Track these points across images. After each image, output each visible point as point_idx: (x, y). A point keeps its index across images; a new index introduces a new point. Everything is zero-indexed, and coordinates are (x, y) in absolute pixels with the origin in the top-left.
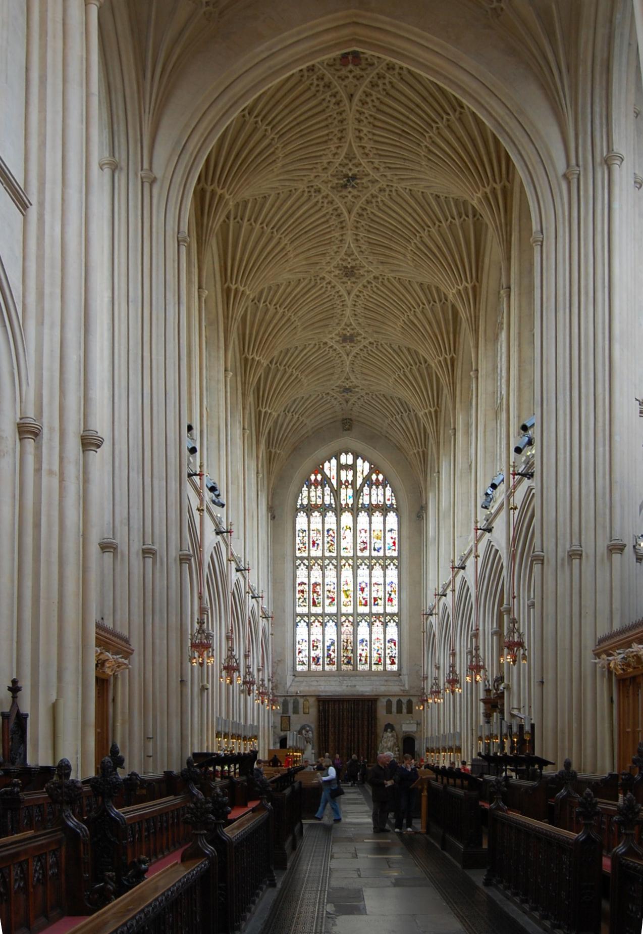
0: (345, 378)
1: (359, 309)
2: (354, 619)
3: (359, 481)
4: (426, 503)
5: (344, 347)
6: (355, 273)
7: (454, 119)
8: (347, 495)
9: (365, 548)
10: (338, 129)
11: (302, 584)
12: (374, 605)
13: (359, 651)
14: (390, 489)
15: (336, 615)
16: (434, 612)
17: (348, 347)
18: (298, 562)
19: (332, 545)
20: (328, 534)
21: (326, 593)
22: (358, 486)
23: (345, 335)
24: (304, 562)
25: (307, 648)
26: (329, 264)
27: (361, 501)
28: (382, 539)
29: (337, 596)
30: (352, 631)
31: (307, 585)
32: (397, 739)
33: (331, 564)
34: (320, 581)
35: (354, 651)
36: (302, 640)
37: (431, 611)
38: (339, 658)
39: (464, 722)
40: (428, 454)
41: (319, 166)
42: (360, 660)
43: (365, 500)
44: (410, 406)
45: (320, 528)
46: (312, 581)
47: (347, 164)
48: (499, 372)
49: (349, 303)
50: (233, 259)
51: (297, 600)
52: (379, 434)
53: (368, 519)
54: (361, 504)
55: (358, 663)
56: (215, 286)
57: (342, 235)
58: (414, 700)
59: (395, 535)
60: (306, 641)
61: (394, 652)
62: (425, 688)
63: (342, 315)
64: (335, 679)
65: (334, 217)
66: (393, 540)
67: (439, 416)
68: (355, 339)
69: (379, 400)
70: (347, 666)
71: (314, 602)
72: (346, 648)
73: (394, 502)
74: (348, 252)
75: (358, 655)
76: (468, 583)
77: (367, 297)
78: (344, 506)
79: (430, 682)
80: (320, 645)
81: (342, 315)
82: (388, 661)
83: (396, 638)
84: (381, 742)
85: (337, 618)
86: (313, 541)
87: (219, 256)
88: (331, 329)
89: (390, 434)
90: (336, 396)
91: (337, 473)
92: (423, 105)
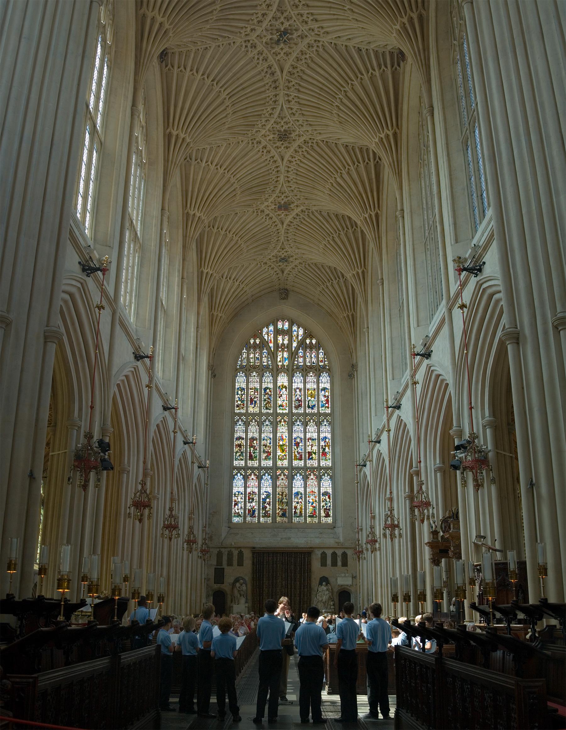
4: (357, 362)
12: (309, 459)
18: (237, 418)
32: (332, 593)
34: (256, 435)
35: (289, 503)
42: (295, 512)
58: (349, 553)
62: (360, 539)
63: (277, 181)
67: (366, 276)
85: (274, 472)
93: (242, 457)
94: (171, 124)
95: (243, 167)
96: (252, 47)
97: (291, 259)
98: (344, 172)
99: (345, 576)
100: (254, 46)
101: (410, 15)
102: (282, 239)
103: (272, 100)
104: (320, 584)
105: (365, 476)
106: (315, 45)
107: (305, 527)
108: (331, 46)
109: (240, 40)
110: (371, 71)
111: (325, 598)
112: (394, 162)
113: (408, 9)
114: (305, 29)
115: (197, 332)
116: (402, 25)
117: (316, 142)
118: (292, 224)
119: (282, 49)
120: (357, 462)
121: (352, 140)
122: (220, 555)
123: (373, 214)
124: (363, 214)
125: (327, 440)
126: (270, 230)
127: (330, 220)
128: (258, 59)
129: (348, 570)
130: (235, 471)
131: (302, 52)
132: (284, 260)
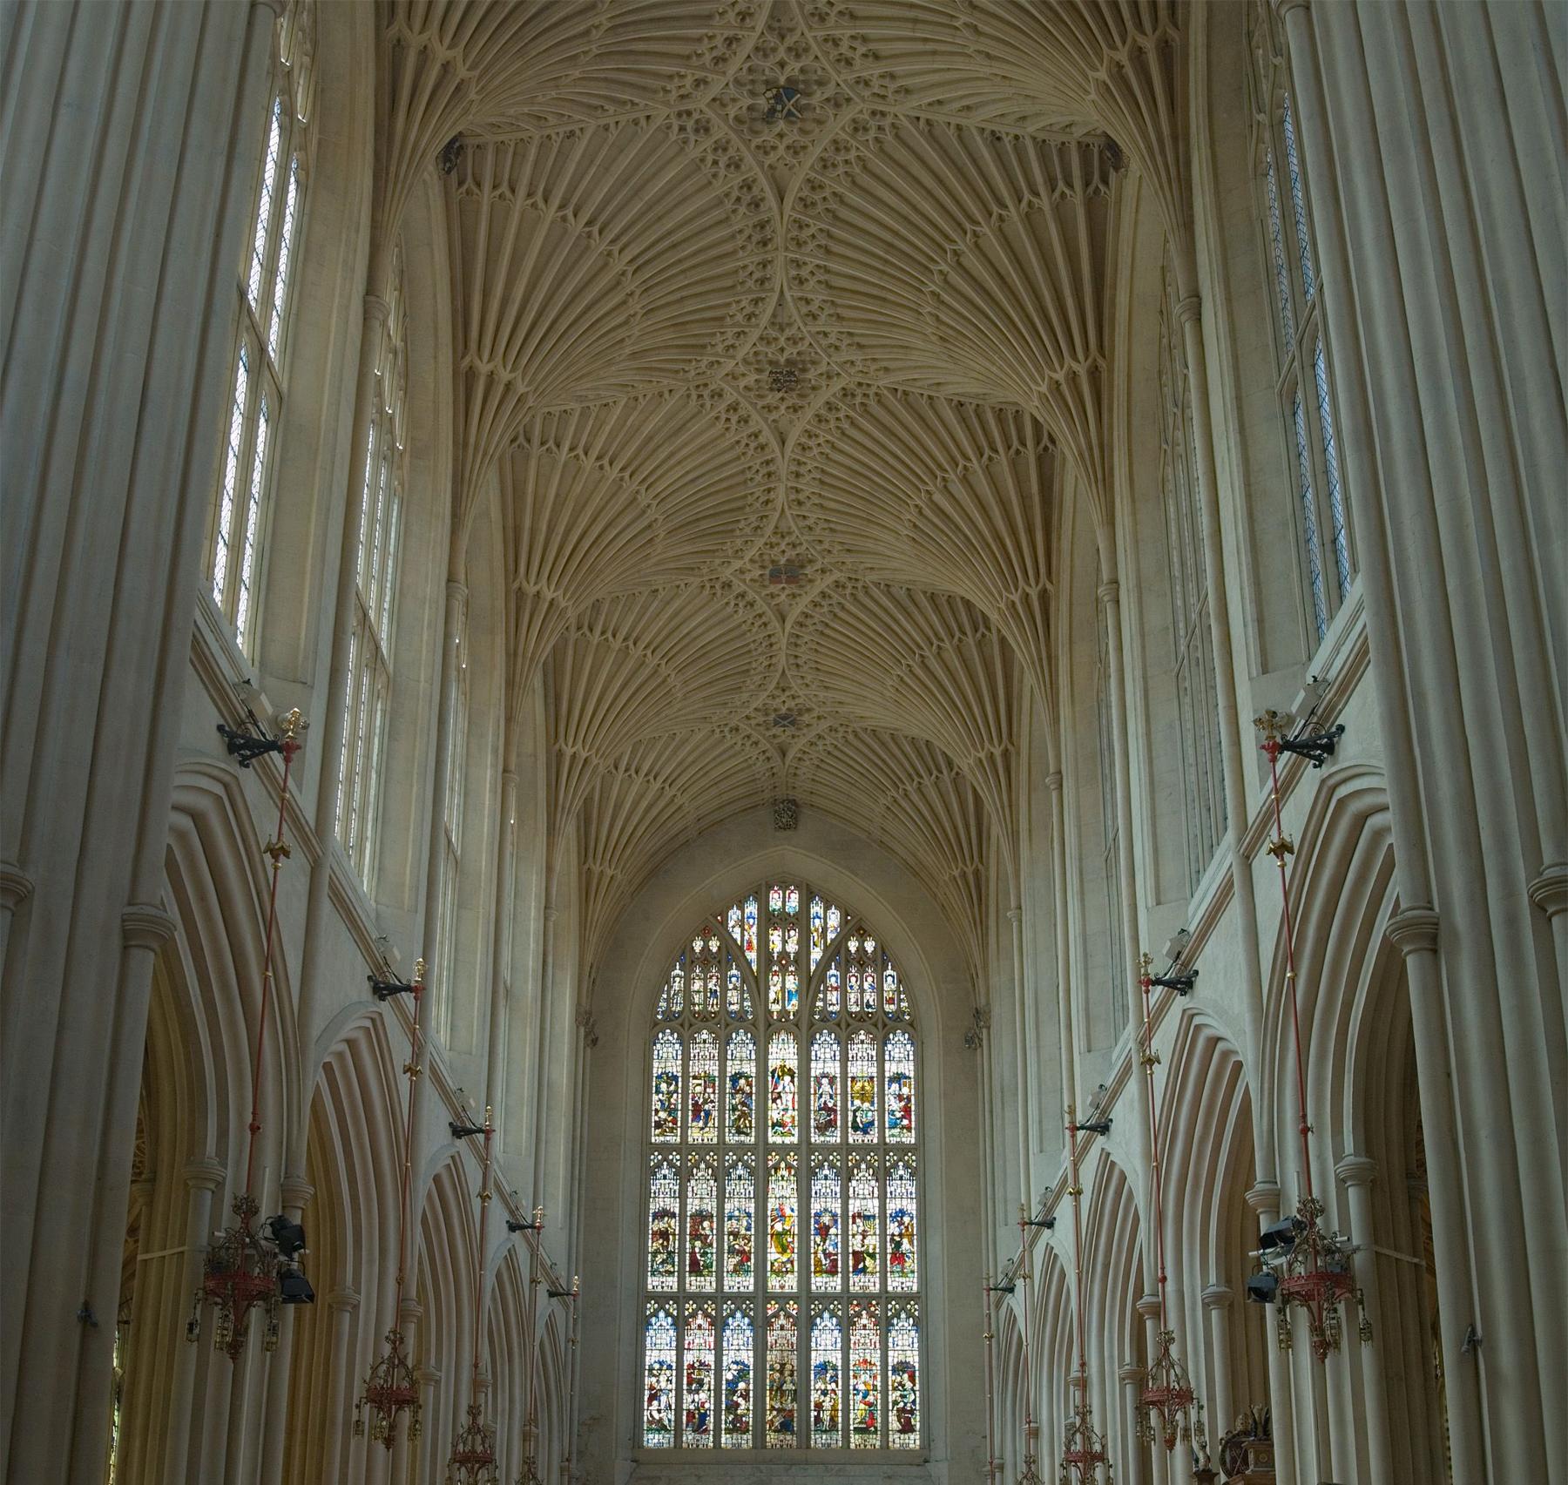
4: (988, 1004)
9: (831, 1124)
12: (857, 1271)
13: (814, 1396)
18: (656, 1157)
19: (744, 1115)
34: (710, 1206)
35: (801, 1395)
36: (661, 1363)
42: (818, 1419)
46: (691, 1209)
60: (670, 1367)
63: (767, 502)
71: (694, 1263)
72: (780, 1388)
80: (709, 1379)
83: (914, 1359)
85: (758, 1308)
86: (696, 1104)
93: (669, 1267)
94: (473, 345)
95: (672, 462)
96: (697, 131)
97: (806, 718)
98: (952, 476)
100: (703, 128)
102: (782, 661)
103: (755, 276)
105: (1012, 1319)
106: (873, 124)
108: (917, 129)
109: (665, 111)
110: (1027, 196)
112: (1090, 449)
115: (546, 919)
117: (876, 394)
118: (809, 622)
119: (781, 136)
120: (988, 1279)
121: (973, 388)
123: (1034, 593)
125: (906, 1219)
126: (749, 638)
127: (912, 609)
128: (715, 163)
130: (651, 1306)
131: (837, 146)
132: (788, 720)
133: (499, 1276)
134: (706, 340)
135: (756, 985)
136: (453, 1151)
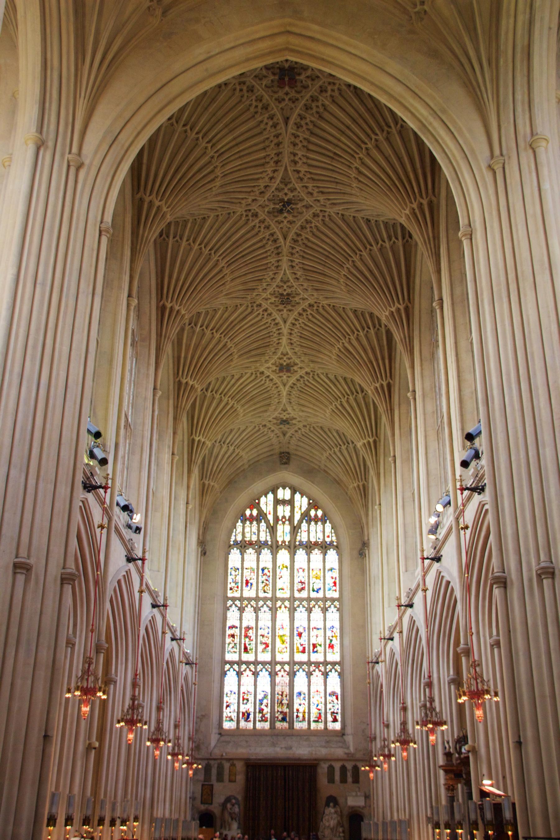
0: (282, 410)
1: (294, 337)
2: (290, 668)
3: (297, 517)
4: (368, 539)
5: (280, 377)
6: (291, 301)
7: (382, 139)
8: (283, 532)
9: (303, 589)
10: (275, 152)
11: (231, 627)
12: (314, 652)
13: (296, 706)
14: (330, 525)
15: (269, 663)
16: (380, 660)
17: (285, 377)
18: (230, 603)
19: (267, 585)
20: (263, 573)
21: (260, 638)
22: (296, 523)
23: (281, 365)
24: (236, 603)
25: (236, 701)
26: (265, 291)
27: (298, 538)
28: (322, 578)
29: (272, 642)
30: (287, 681)
31: (239, 628)
32: (341, 816)
33: (265, 606)
34: (253, 624)
35: (290, 705)
37: (378, 659)
38: (273, 713)
39: (421, 795)
40: (368, 487)
41: (256, 189)
42: (297, 716)
43: (303, 537)
44: (349, 437)
45: (255, 566)
46: (244, 625)
47: (283, 189)
48: (437, 391)
49: (285, 331)
50: (170, 277)
51: (227, 645)
52: (317, 467)
53: (306, 557)
54: (299, 542)
55: (295, 719)
56: (150, 303)
57: (278, 261)
59: (336, 574)
60: (235, 693)
61: (336, 707)
63: (278, 343)
64: (268, 738)
65: (270, 243)
66: (333, 580)
68: (292, 368)
69: (316, 433)
70: (282, 723)
73: (334, 539)
74: (284, 279)
75: (295, 711)
76: (417, 623)
77: (303, 325)
78: (280, 543)
79: (379, 743)
80: (251, 698)
81: (278, 343)
82: (330, 718)
83: (338, 691)
84: (322, 820)
87: (157, 272)
88: (267, 358)
89: (328, 468)
90: (273, 428)
91: (274, 509)
92: (353, 126)
93: (235, 650)
97: (294, 422)
98: (352, 337)
99: (357, 796)
100: (256, 215)
101: (419, 201)
102: (284, 400)
103: (274, 265)
104: (327, 805)
105: (378, 676)
106: (321, 214)
107: (309, 734)
108: (338, 217)
109: (240, 210)
110: (380, 242)
111: (333, 823)
113: (417, 195)
114: (310, 200)
115: (187, 508)
116: (412, 211)
117: (322, 306)
118: (295, 387)
120: (368, 658)
121: (359, 306)
122: (207, 769)
124: (373, 383)
125: (334, 630)
126: (271, 392)
127: (337, 383)
129: (359, 788)
130: (227, 667)
132: (285, 422)
133: (147, 629)
134: (255, 287)
135: (272, 530)
136: (127, 569)
